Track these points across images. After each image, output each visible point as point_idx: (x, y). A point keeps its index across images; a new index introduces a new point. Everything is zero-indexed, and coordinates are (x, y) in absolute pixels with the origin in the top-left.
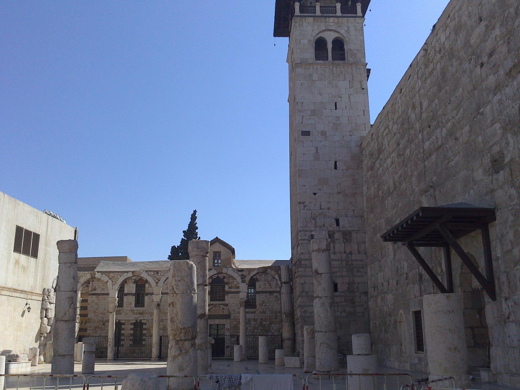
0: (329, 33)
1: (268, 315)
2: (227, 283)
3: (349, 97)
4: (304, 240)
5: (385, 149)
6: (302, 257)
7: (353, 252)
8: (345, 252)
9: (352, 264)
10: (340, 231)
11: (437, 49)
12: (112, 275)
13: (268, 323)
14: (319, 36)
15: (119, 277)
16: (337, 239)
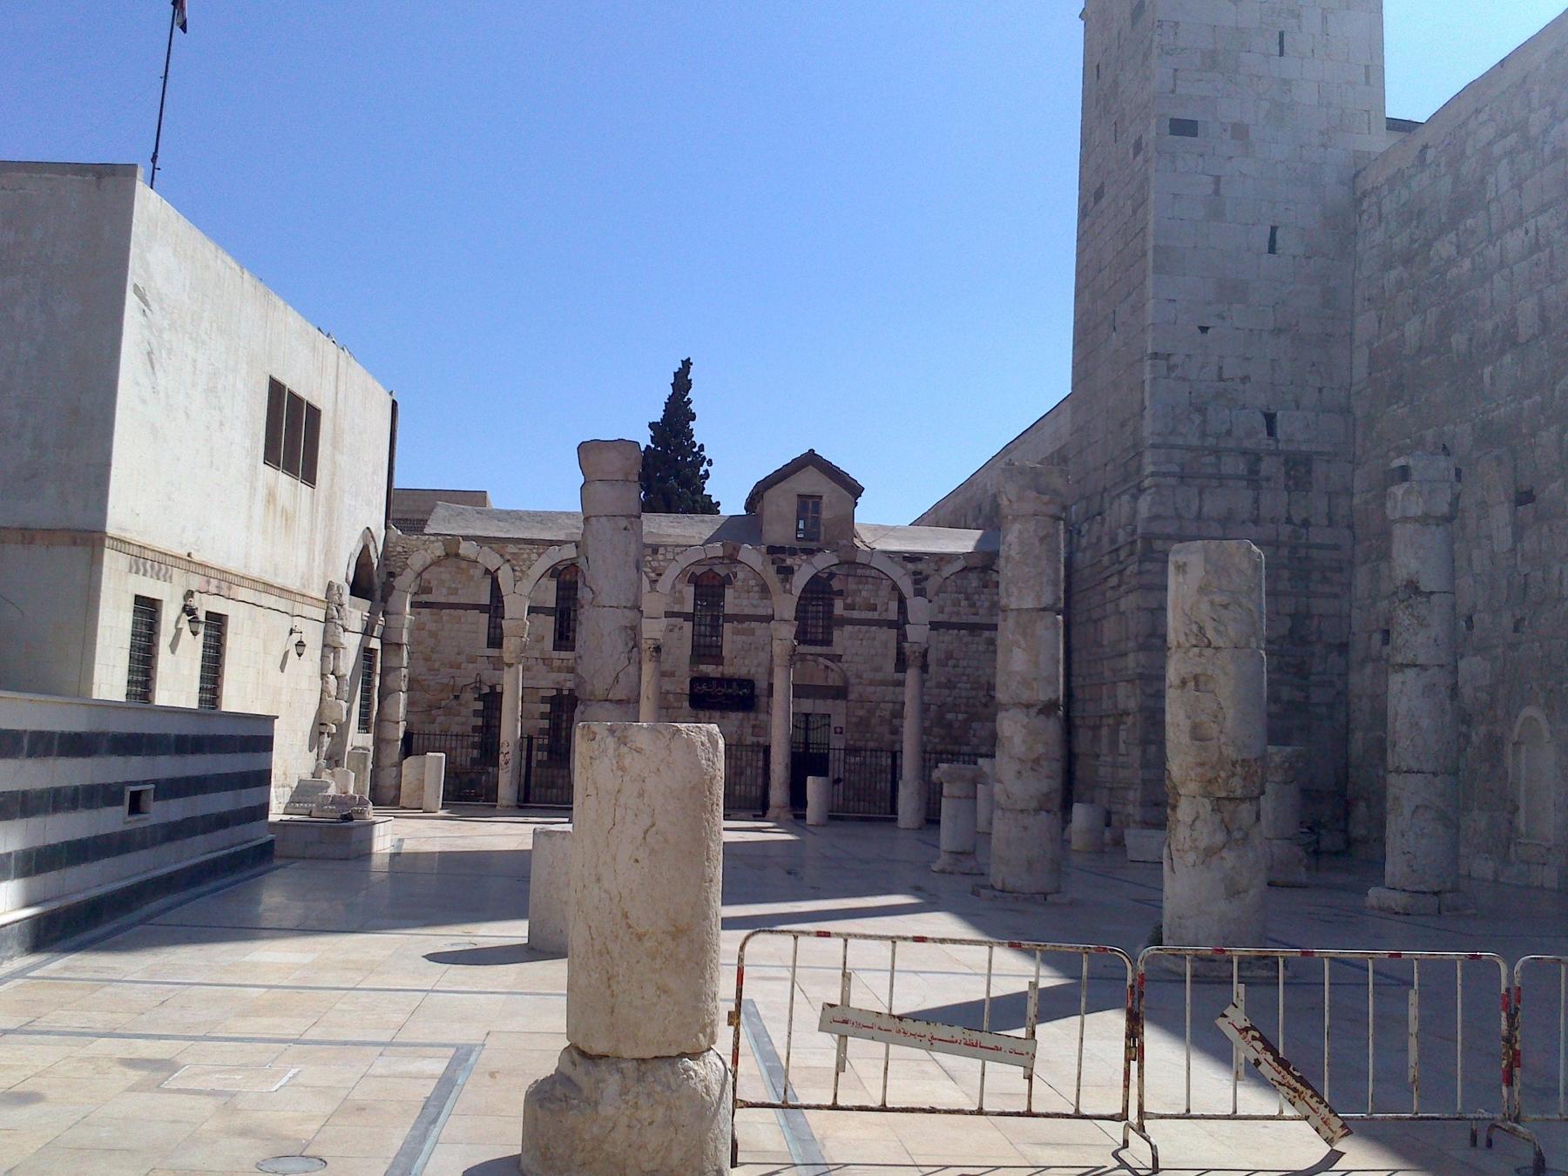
1: (964, 694)
2: (840, 593)
3: (1325, 19)
4: (1165, 475)
6: (1156, 527)
7: (1312, 520)
8: (1289, 520)
10: (1277, 453)
12: (511, 548)
13: (961, 717)
15: (534, 556)
16: (1268, 479)
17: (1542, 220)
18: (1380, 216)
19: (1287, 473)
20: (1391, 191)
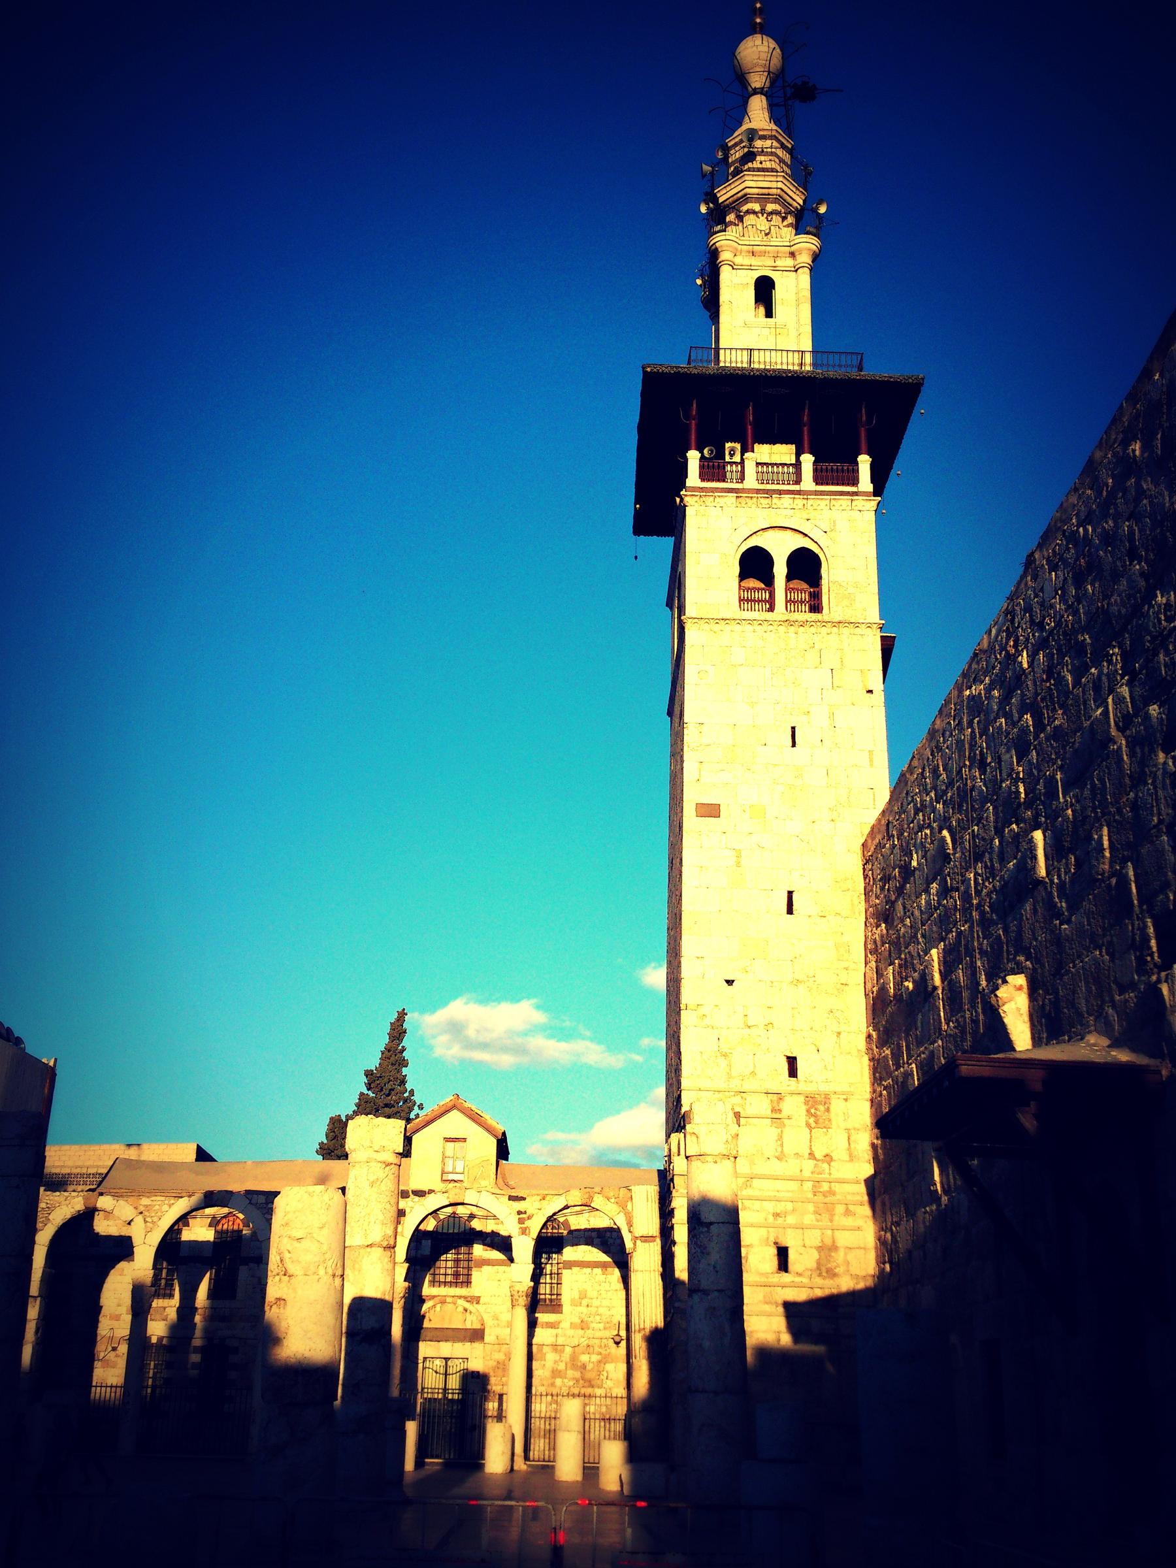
8: (812, 1155)
9: (832, 1193)
13: (595, 1358)
15: (165, 1207)
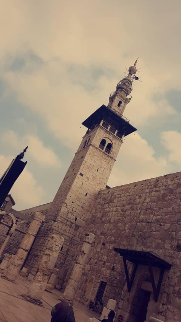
0: (109, 140)
2: (3, 219)
5: (115, 202)
7: (76, 235)
9: (73, 241)
11: (165, 184)
13: (13, 246)
14: (105, 139)
16: (72, 227)
17: (119, 208)
18: (101, 198)
19: (75, 227)
20: (103, 195)
